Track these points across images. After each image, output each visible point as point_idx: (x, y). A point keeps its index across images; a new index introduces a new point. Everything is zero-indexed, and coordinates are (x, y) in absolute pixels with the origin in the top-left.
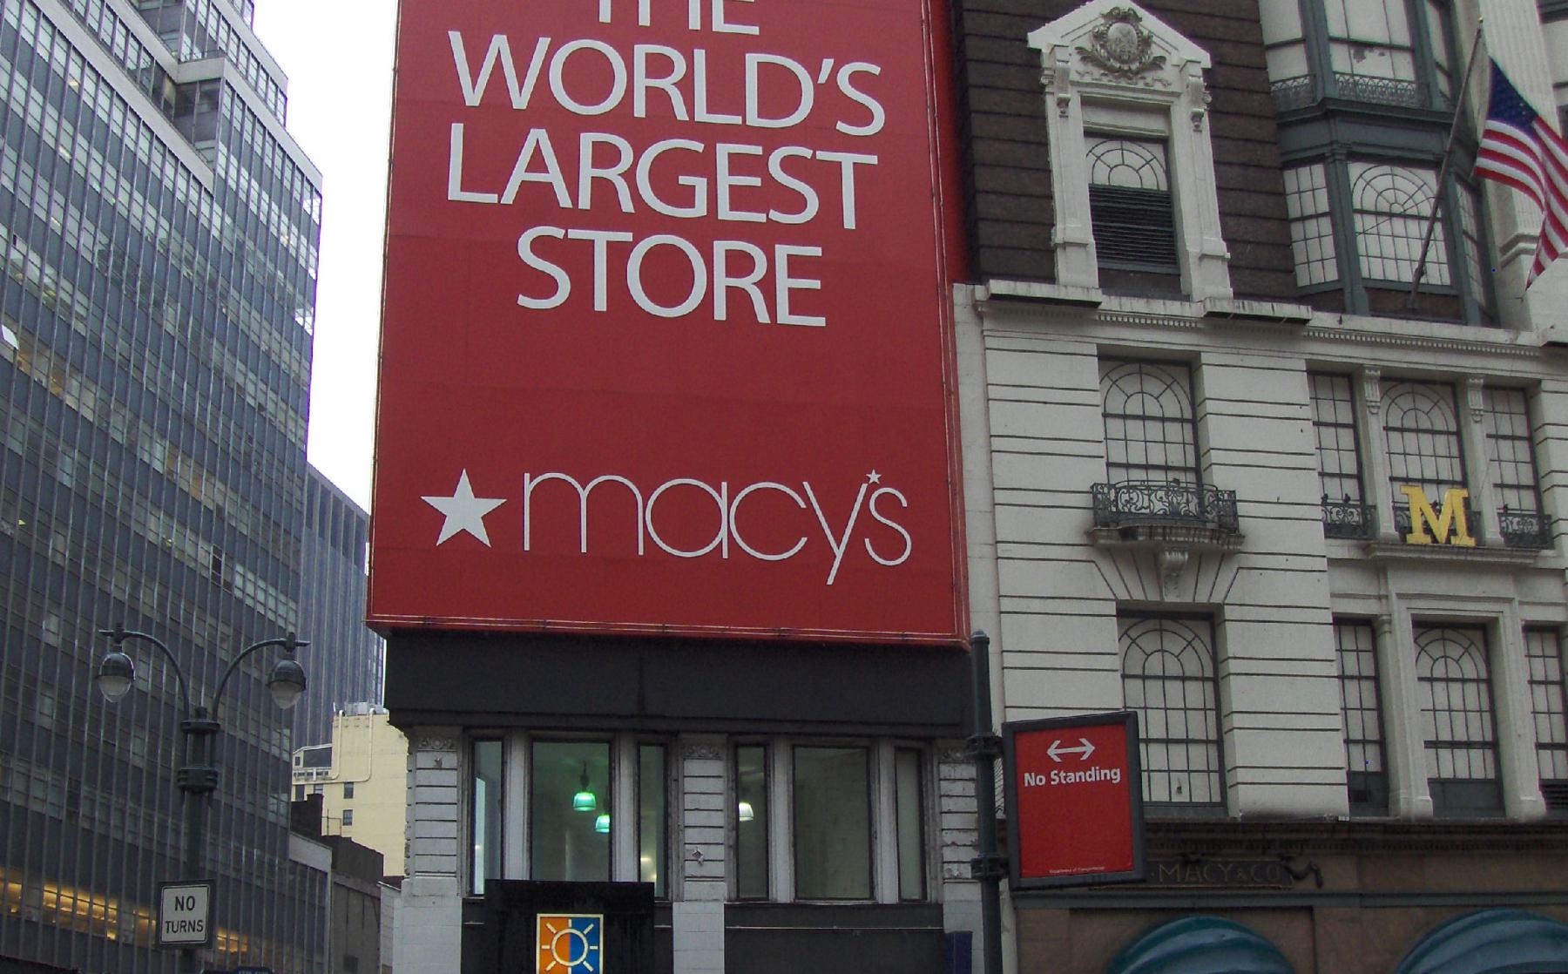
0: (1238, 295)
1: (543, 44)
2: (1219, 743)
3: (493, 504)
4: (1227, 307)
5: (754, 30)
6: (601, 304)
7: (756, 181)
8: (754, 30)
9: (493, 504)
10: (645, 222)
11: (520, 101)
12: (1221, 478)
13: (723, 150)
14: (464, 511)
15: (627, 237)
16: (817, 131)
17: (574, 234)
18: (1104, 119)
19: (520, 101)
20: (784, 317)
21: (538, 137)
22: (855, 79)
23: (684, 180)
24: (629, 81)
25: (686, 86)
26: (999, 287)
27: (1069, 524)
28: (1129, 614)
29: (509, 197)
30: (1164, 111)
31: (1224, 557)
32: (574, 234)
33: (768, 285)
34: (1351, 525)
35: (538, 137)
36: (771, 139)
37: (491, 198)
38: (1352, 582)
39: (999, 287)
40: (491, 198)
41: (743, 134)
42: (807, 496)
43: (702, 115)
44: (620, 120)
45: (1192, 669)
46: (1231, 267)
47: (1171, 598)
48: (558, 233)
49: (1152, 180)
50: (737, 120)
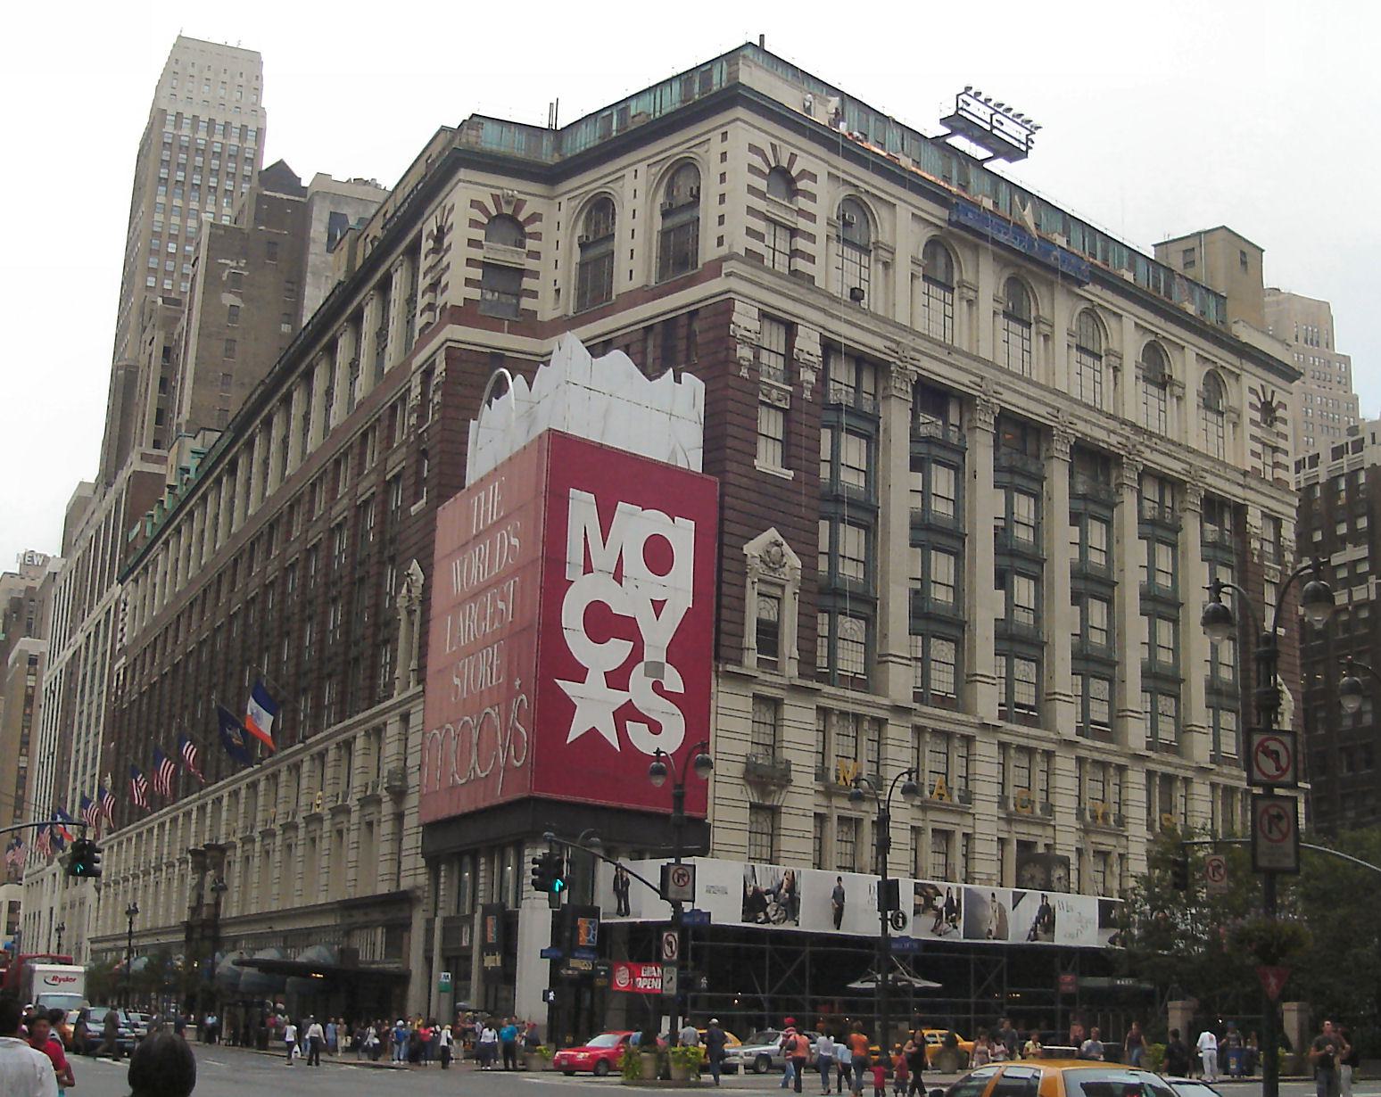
0: (801, 675)
4: (798, 682)
12: (787, 754)
18: (764, 589)
26: (730, 668)
27: (737, 770)
28: (753, 806)
30: (783, 587)
31: (782, 787)
34: (821, 775)
38: (821, 800)
39: (730, 668)
45: (765, 830)
46: (799, 661)
47: (767, 803)
49: (773, 617)
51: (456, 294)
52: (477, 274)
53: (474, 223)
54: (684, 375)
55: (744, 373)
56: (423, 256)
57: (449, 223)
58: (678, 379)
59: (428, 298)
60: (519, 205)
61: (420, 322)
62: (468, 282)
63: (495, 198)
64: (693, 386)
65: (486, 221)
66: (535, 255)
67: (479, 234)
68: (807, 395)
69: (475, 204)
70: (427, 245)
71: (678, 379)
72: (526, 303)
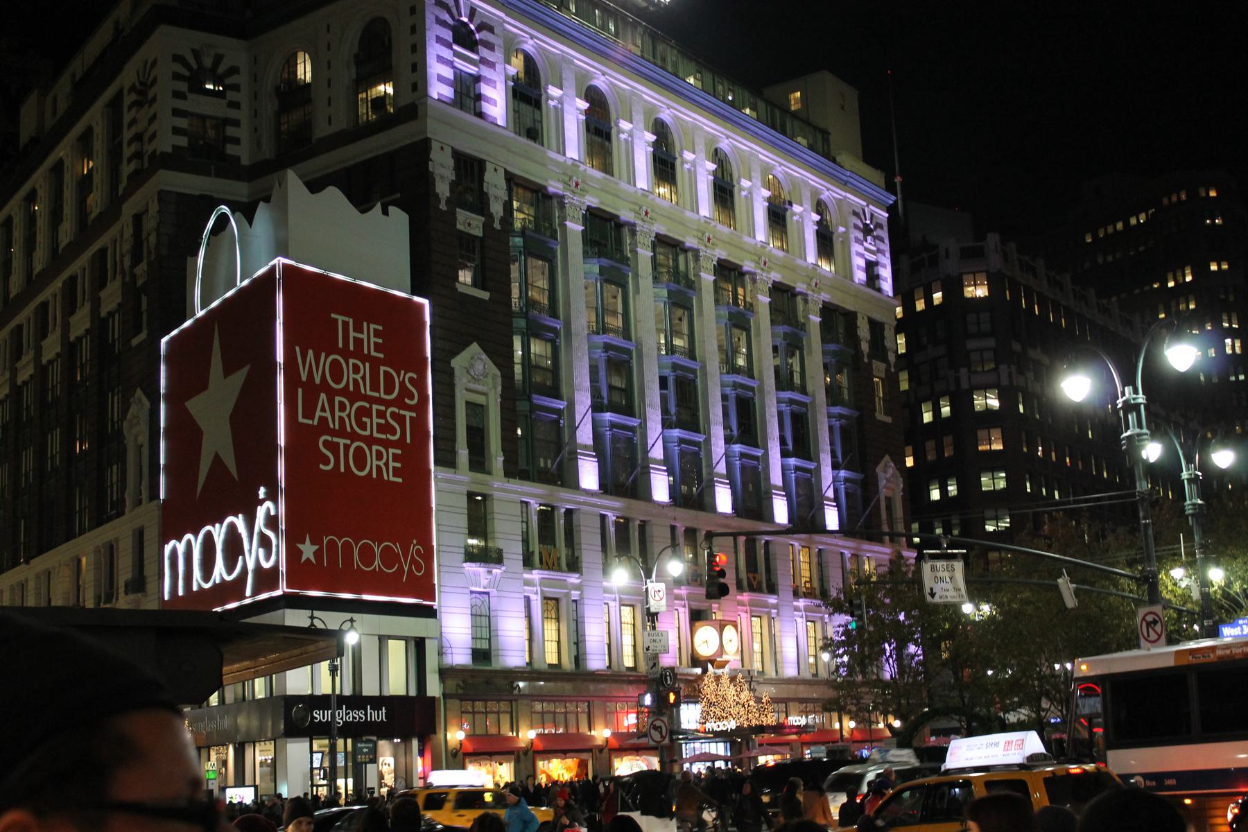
1: (323, 355)
2: (489, 640)
3: (316, 547)
5: (382, 356)
6: (342, 470)
7: (382, 421)
8: (382, 356)
9: (316, 547)
10: (354, 437)
11: (318, 381)
13: (375, 407)
14: (308, 550)
15: (348, 442)
16: (399, 403)
17: (335, 440)
19: (318, 381)
20: (392, 479)
21: (323, 396)
22: (411, 379)
23: (364, 419)
24: (349, 376)
25: (364, 378)
29: (316, 423)
32: (335, 440)
33: (387, 464)
35: (323, 396)
36: (388, 404)
37: (310, 422)
40: (310, 422)
41: (380, 401)
42: (397, 549)
43: (369, 393)
44: (344, 392)
48: (329, 438)
50: (377, 395)
51: (166, 142)
52: (183, 123)
53: (177, 76)
54: (392, 209)
55: (443, 207)
56: (125, 109)
57: (151, 77)
58: (385, 212)
59: (133, 148)
60: (218, 59)
61: (127, 169)
62: (177, 131)
63: (196, 54)
64: (399, 220)
65: (187, 73)
66: (235, 105)
67: (183, 87)
68: (497, 225)
69: (178, 59)
70: (128, 99)
71: (385, 212)
72: (231, 149)
